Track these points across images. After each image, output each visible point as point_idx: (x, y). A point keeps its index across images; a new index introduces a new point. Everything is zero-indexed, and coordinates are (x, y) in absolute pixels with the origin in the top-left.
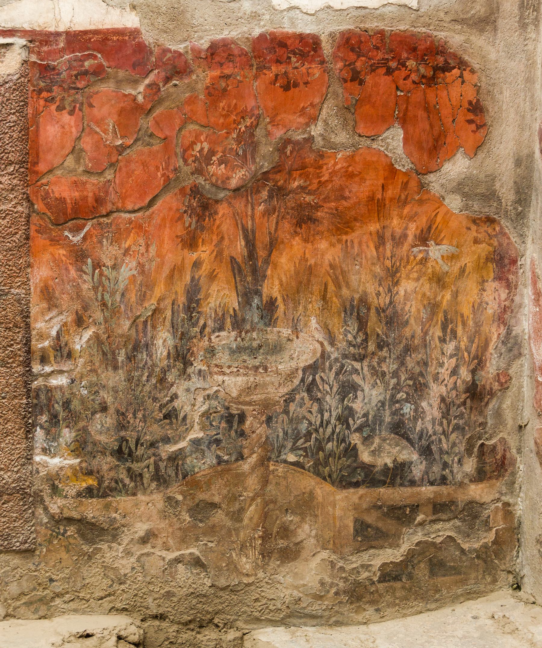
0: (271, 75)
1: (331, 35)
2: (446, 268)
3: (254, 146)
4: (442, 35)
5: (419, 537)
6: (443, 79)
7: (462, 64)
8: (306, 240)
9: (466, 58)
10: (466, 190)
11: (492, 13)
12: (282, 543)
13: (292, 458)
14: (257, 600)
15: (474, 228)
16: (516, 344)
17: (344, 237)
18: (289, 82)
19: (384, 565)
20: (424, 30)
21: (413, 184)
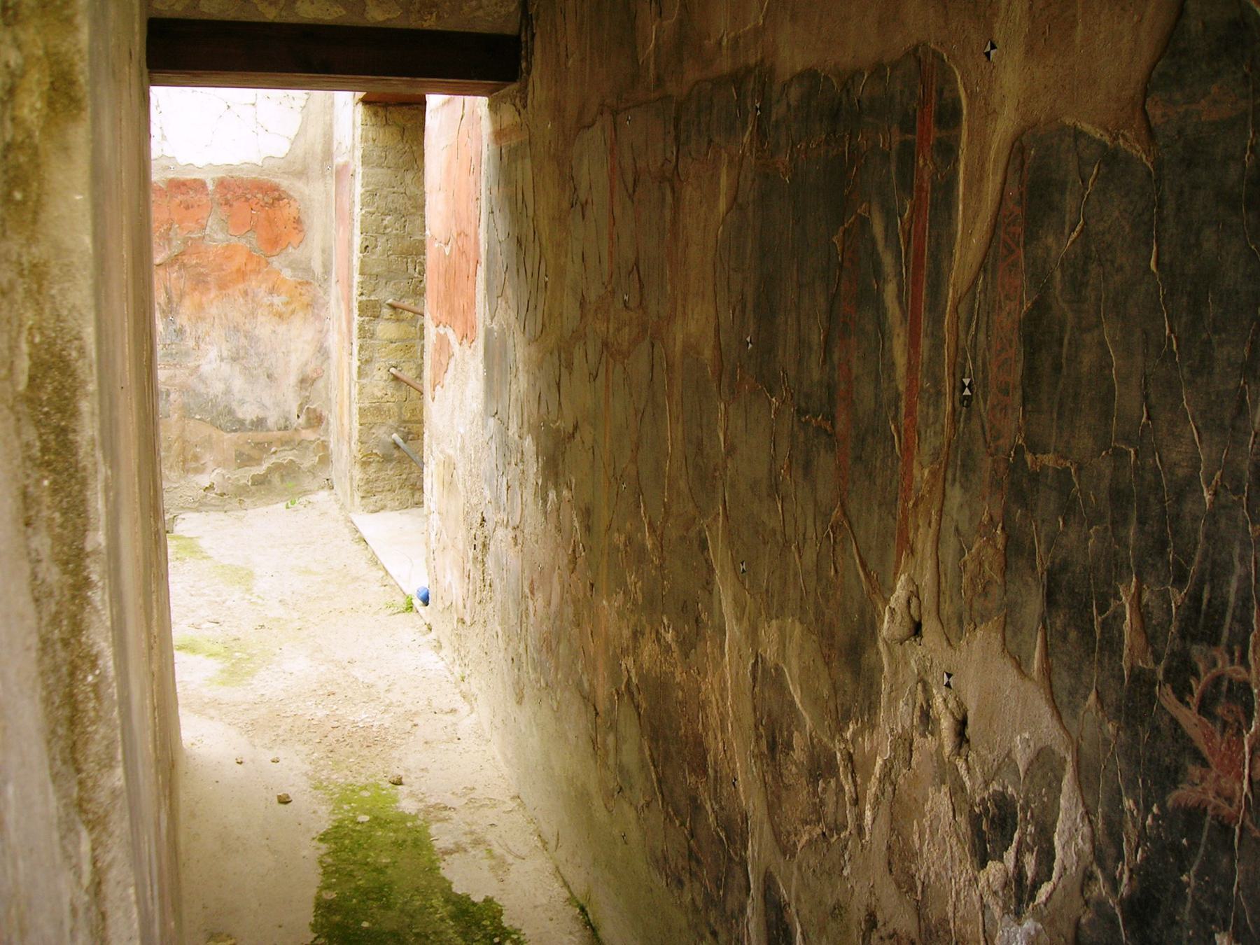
0: (178, 201)
1: (213, 180)
2: (284, 309)
3: (169, 240)
4: (277, 180)
5: (274, 459)
6: (279, 204)
7: (290, 197)
8: (202, 293)
9: (292, 194)
10: (294, 266)
11: (305, 169)
12: (193, 465)
13: (198, 417)
14: (181, 497)
15: (299, 287)
16: (326, 352)
17: (224, 292)
18: (188, 206)
19: (254, 475)
20: (266, 177)
21: (263, 262)
